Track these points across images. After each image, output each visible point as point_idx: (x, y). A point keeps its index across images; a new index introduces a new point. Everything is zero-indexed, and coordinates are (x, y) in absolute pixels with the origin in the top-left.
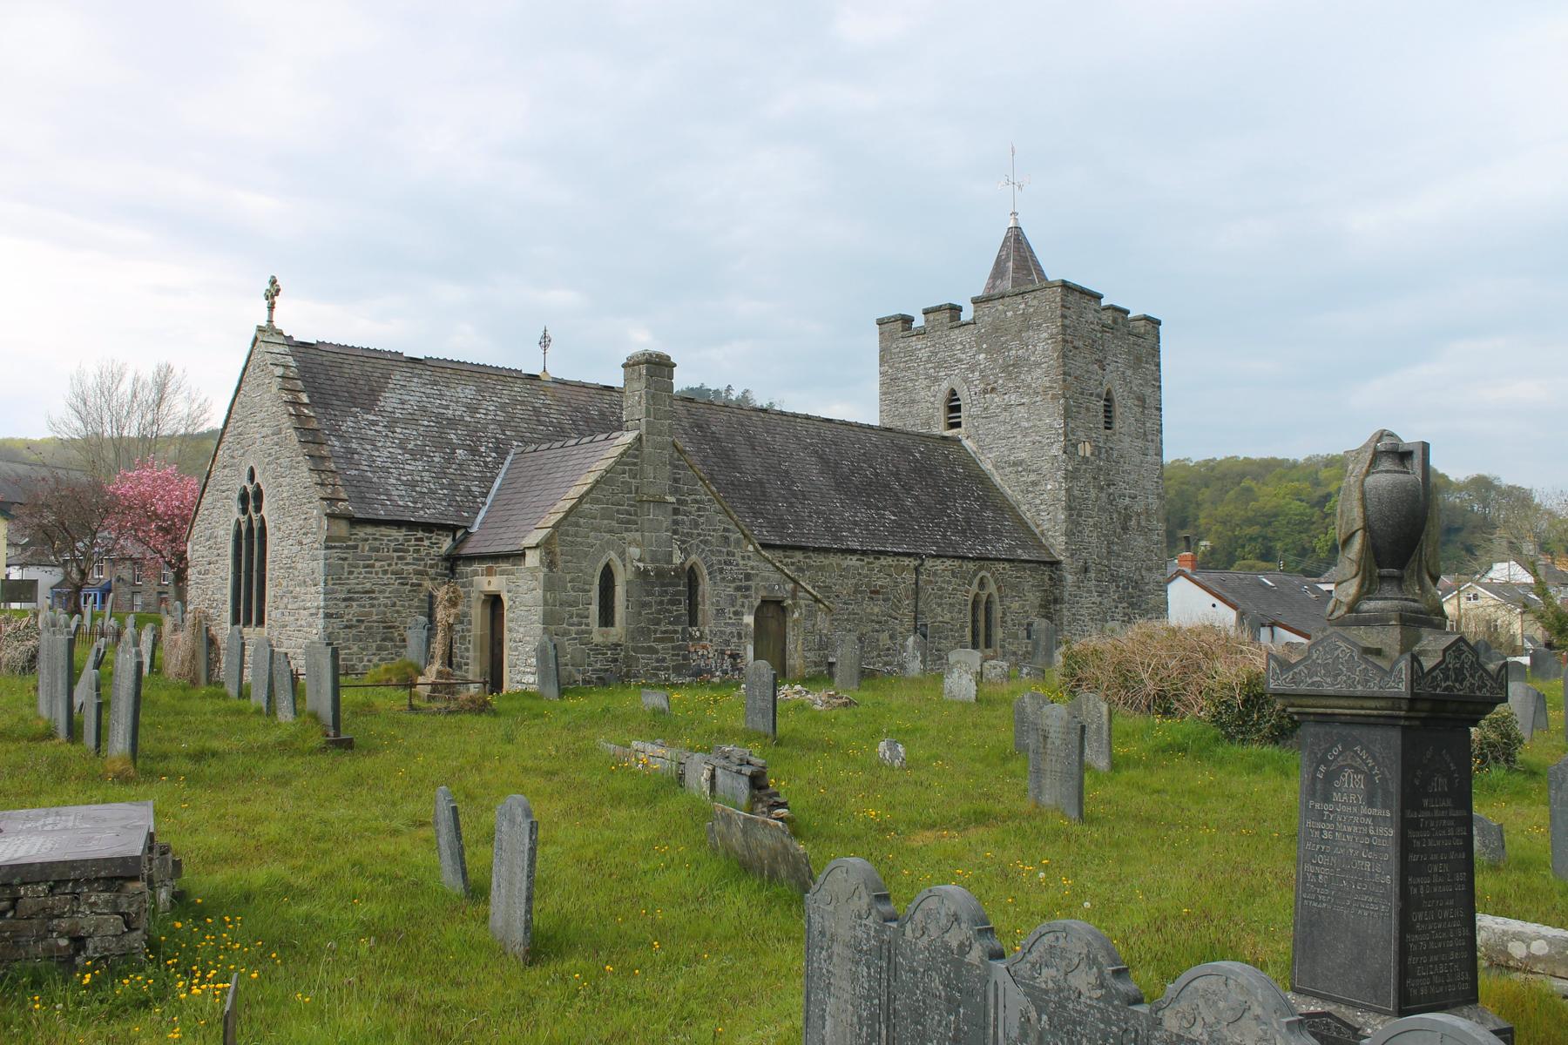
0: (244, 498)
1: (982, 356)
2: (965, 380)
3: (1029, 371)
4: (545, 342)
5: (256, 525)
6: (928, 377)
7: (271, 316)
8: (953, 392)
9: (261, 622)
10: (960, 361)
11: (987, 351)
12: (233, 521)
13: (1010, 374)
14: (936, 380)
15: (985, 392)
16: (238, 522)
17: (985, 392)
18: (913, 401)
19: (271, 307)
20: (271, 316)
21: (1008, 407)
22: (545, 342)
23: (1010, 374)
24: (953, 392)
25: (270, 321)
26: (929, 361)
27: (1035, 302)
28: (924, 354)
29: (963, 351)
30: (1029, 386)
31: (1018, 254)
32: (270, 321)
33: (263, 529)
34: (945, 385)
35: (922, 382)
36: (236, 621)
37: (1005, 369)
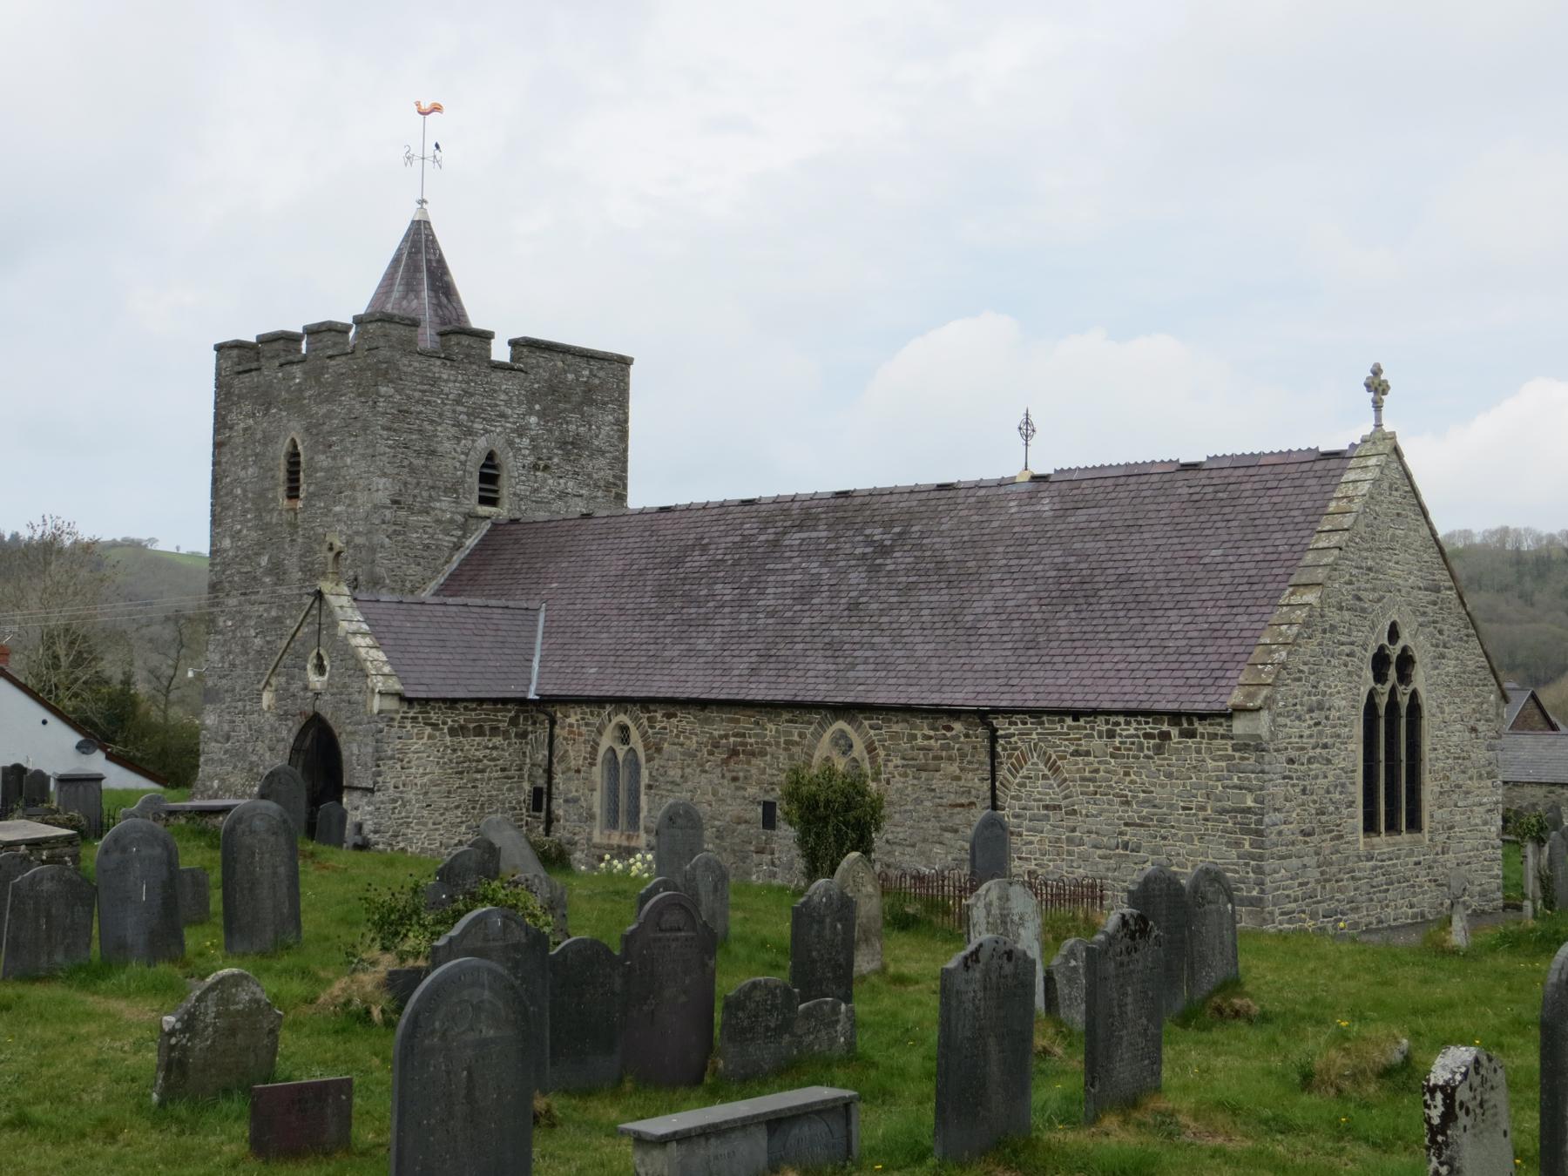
0: (1380, 662)
1: (533, 420)
2: (511, 443)
3: (591, 457)
4: (1027, 429)
5: (1404, 701)
6: (458, 424)
7: (1378, 418)
8: (491, 456)
9: (1414, 824)
10: (503, 415)
11: (542, 415)
12: (1364, 692)
13: (568, 453)
14: (470, 432)
15: (536, 467)
16: (1372, 695)
17: (536, 467)
18: (433, 453)
19: (1377, 406)
20: (1378, 418)
21: (563, 495)
22: (1027, 429)
23: (568, 453)
24: (491, 456)
25: (1378, 425)
26: (458, 402)
27: (601, 374)
28: (453, 389)
29: (508, 403)
30: (590, 476)
31: (420, 259)
32: (1378, 425)
33: (1415, 708)
34: (482, 443)
35: (445, 430)
36: (1370, 826)
37: (563, 444)
